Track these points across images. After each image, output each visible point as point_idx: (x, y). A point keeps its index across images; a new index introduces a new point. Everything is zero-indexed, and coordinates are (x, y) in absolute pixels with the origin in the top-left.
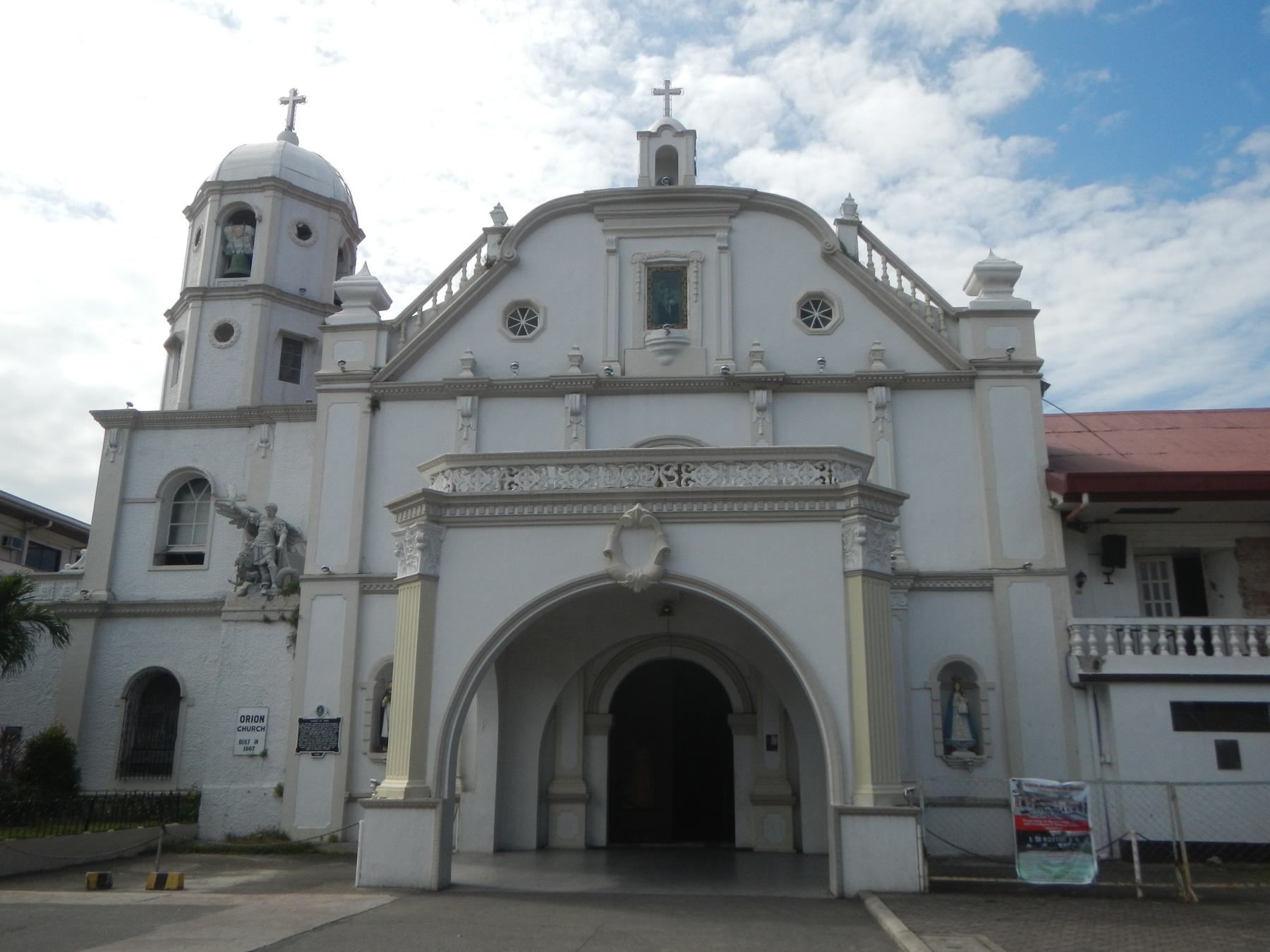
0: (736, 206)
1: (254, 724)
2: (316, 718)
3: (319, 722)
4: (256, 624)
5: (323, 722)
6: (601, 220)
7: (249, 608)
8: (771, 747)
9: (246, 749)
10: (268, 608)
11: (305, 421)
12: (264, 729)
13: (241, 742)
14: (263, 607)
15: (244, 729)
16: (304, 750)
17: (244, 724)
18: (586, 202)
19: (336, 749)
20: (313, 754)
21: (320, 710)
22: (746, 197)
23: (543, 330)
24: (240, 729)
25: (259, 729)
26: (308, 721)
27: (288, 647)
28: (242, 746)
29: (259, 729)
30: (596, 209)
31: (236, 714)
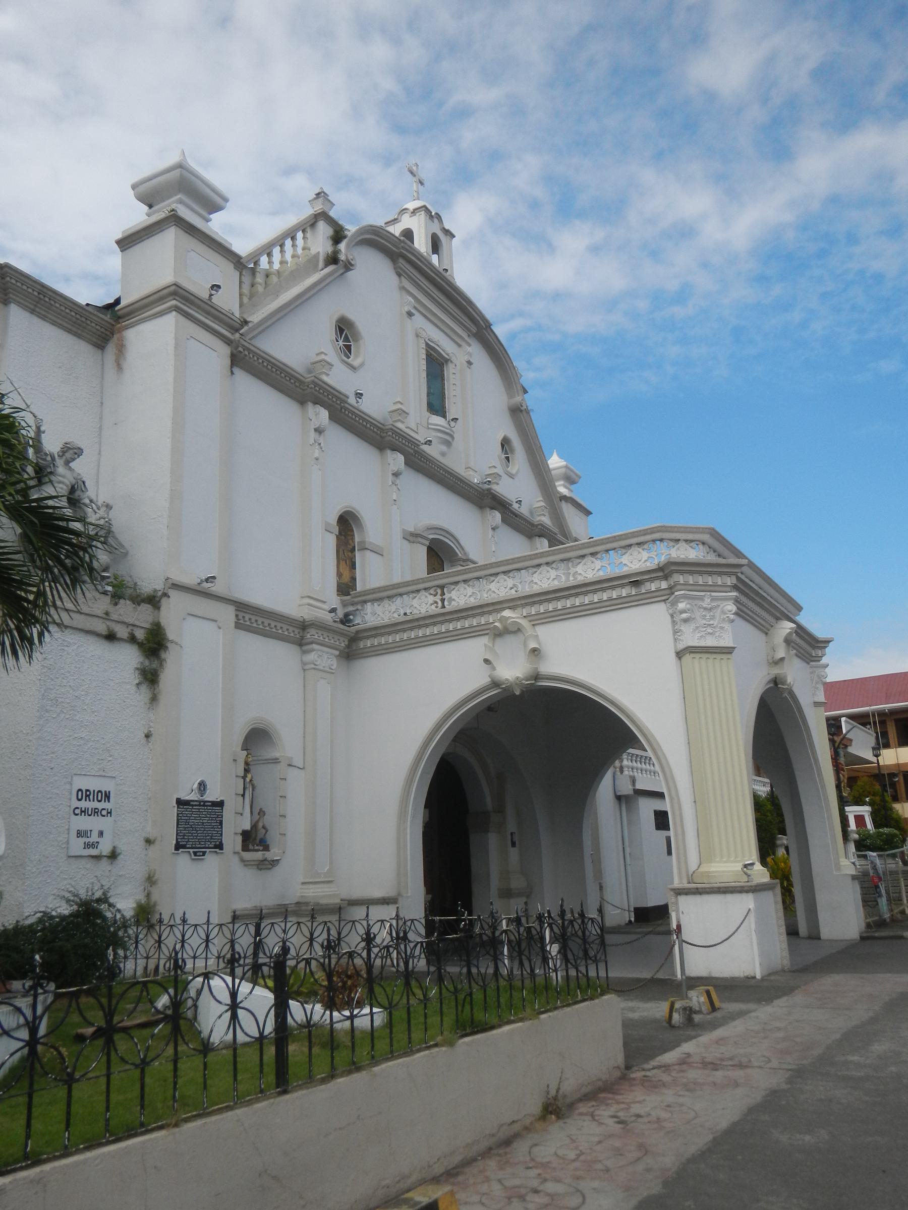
0: (474, 330)
2: (196, 799)
3: (199, 805)
4: (92, 639)
5: (204, 805)
6: (399, 275)
8: (513, 844)
9: (88, 846)
10: (114, 617)
11: (54, 323)
12: (110, 813)
13: (79, 834)
14: (107, 614)
15: (84, 812)
16: (184, 847)
17: (84, 804)
18: (397, 248)
19: (220, 846)
21: (202, 786)
22: (484, 326)
24: (77, 811)
25: (104, 813)
26: (187, 803)
27: (137, 684)
28: (82, 840)
29: (104, 813)
30: (401, 260)
31: (68, 787)
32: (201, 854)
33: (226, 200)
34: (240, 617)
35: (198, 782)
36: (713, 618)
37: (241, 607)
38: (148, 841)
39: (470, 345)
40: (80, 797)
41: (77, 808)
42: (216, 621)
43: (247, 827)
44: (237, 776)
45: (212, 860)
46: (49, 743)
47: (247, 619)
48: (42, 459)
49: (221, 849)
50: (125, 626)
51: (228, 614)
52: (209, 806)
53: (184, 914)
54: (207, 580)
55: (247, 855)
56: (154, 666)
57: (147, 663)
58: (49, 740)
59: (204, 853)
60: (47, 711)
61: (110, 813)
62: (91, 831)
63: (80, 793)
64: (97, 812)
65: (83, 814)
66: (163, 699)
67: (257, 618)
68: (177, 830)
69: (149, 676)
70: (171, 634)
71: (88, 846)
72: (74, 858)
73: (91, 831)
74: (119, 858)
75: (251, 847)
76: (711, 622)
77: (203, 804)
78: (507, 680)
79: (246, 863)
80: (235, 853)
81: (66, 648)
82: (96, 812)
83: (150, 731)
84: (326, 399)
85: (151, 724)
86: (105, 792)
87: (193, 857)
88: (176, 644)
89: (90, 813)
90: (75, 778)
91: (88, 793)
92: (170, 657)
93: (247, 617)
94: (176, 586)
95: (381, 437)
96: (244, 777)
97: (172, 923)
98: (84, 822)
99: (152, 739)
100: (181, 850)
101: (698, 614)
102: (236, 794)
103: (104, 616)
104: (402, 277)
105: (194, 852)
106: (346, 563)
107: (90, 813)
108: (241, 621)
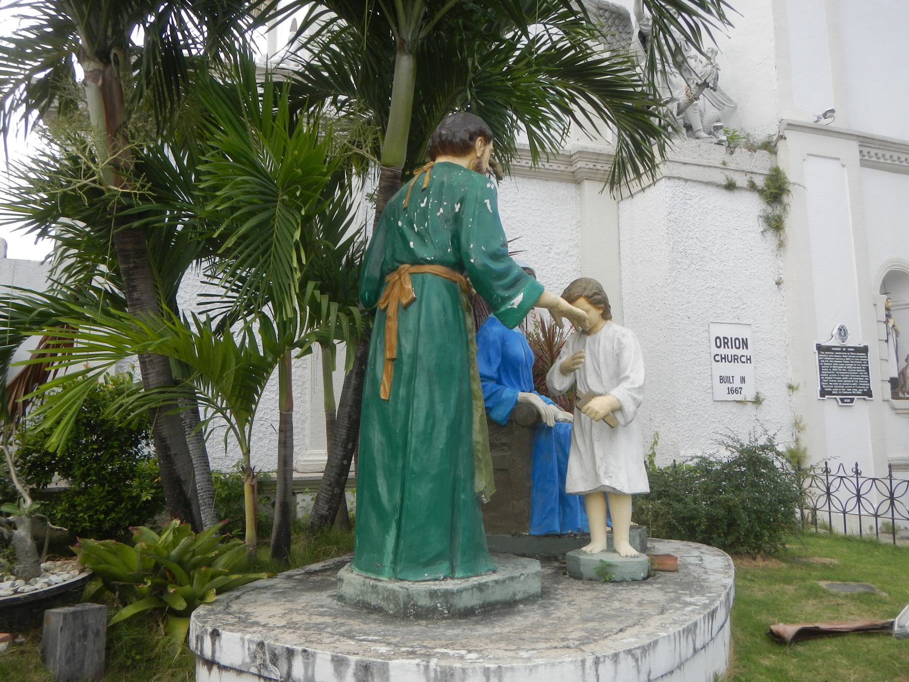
1: (734, 351)
2: (838, 345)
3: (842, 351)
4: (712, 190)
5: (847, 351)
7: (704, 162)
9: (731, 391)
10: (732, 166)
12: (750, 359)
13: (722, 379)
14: (724, 164)
15: (724, 358)
16: (830, 393)
17: (723, 351)
19: (869, 393)
20: (842, 400)
21: (842, 331)
24: (718, 358)
25: (744, 359)
26: (829, 349)
29: (744, 359)
32: (849, 401)
34: (865, 153)
35: (838, 327)
37: (865, 141)
38: (791, 387)
40: (718, 345)
41: (718, 355)
42: (838, 159)
43: (895, 374)
44: (878, 321)
45: (859, 405)
46: (683, 294)
47: (873, 154)
48: (645, 25)
49: (871, 396)
50: (744, 174)
51: (852, 150)
52: (852, 352)
53: (857, 465)
54: (825, 116)
55: (898, 403)
56: (777, 212)
57: (769, 210)
58: (683, 291)
59: (852, 400)
60: (678, 263)
61: (749, 359)
62: (733, 377)
63: (718, 340)
64: (737, 359)
65: (723, 360)
66: (790, 244)
67: (884, 152)
68: (821, 377)
69: (773, 223)
70: (791, 175)
71: (731, 391)
72: (720, 403)
73: (733, 377)
74: (763, 403)
75: (901, 395)
77: (845, 350)
79: (898, 412)
80: (884, 401)
81: (688, 201)
82: (735, 358)
83: (781, 278)
85: (781, 271)
86: (743, 339)
87: (841, 404)
88: (799, 185)
89: (730, 360)
90: (712, 326)
91: (726, 341)
92: (792, 200)
93: (873, 152)
94: (792, 126)
96: (887, 322)
97: (841, 474)
98: (726, 369)
99: (782, 286)
100: (827, 396)
102: (880, 340)
103: (722, 166)
105: (840, 399)
107: (730, 360)
108: (867, 158)
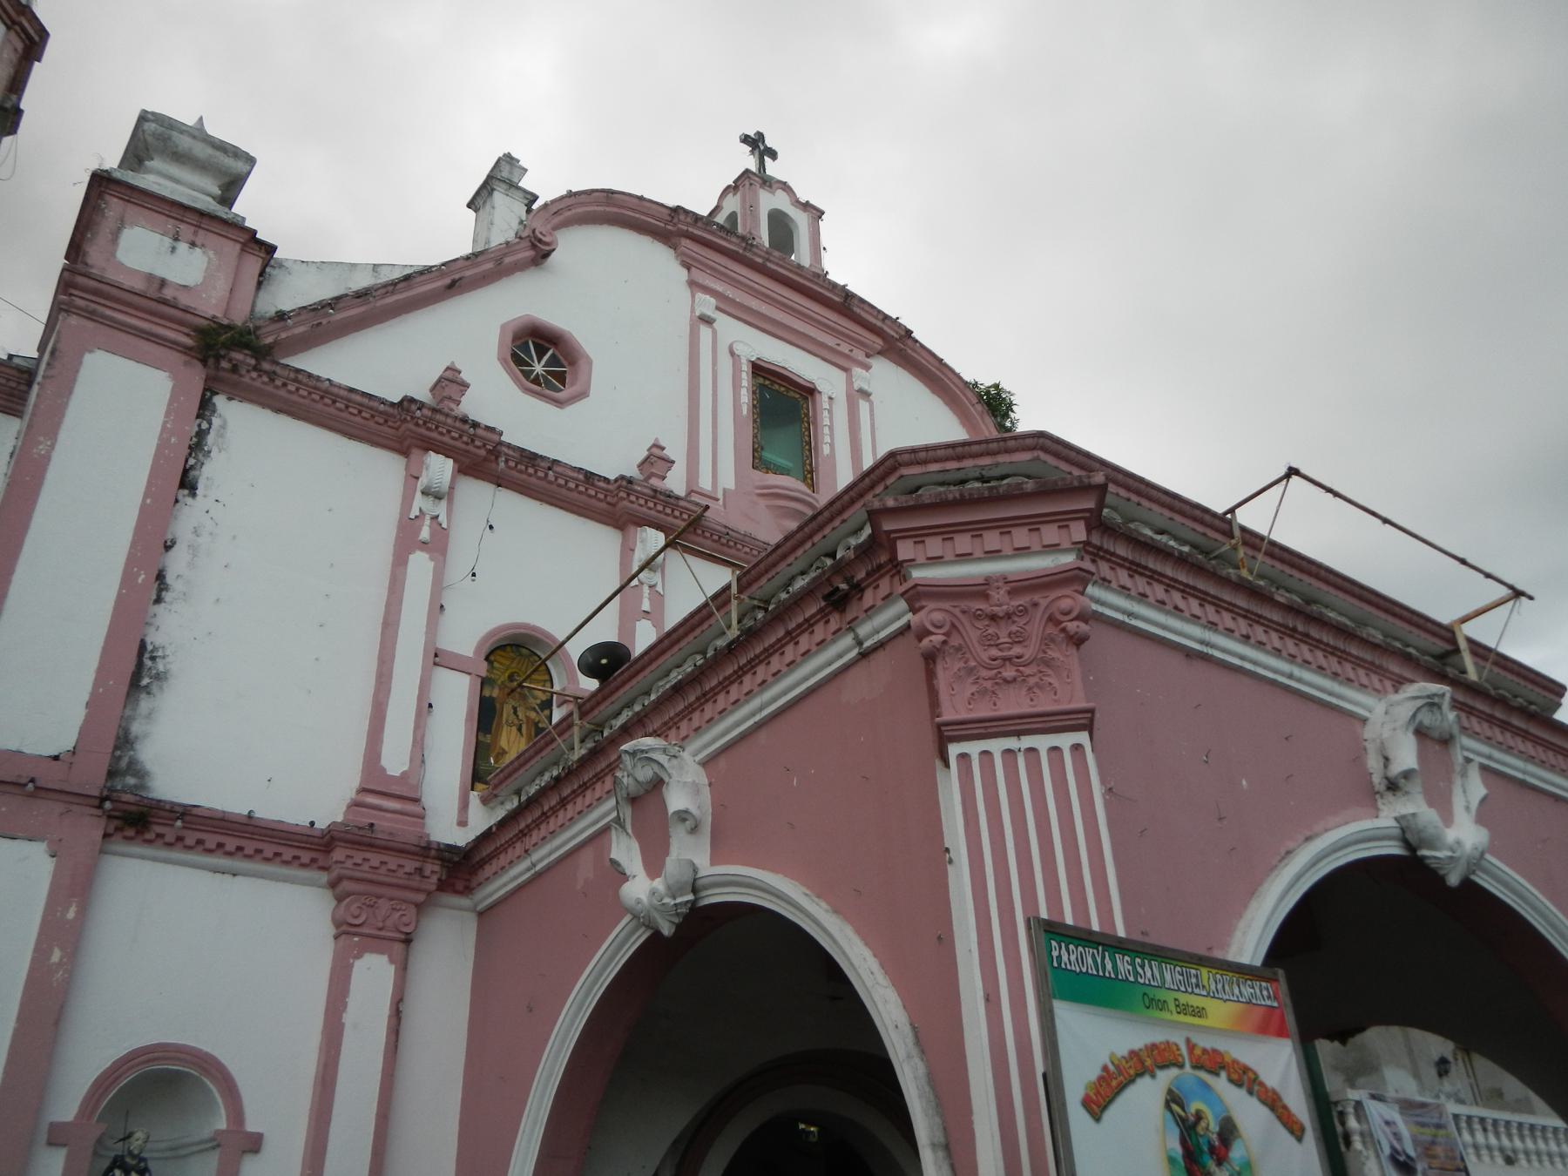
0: (878, 343)
22: (898, 337)
23: (583, 394)
30: (686, 242)
33: (251, 161)
36: (1018, 639)
39: (867, 367)
76: (1017, 650)
78: (639, 901)
84: (446, 439)
95: (609, 503)
101: (972, 633)
104: (693, 269)
106: (520, 729)
